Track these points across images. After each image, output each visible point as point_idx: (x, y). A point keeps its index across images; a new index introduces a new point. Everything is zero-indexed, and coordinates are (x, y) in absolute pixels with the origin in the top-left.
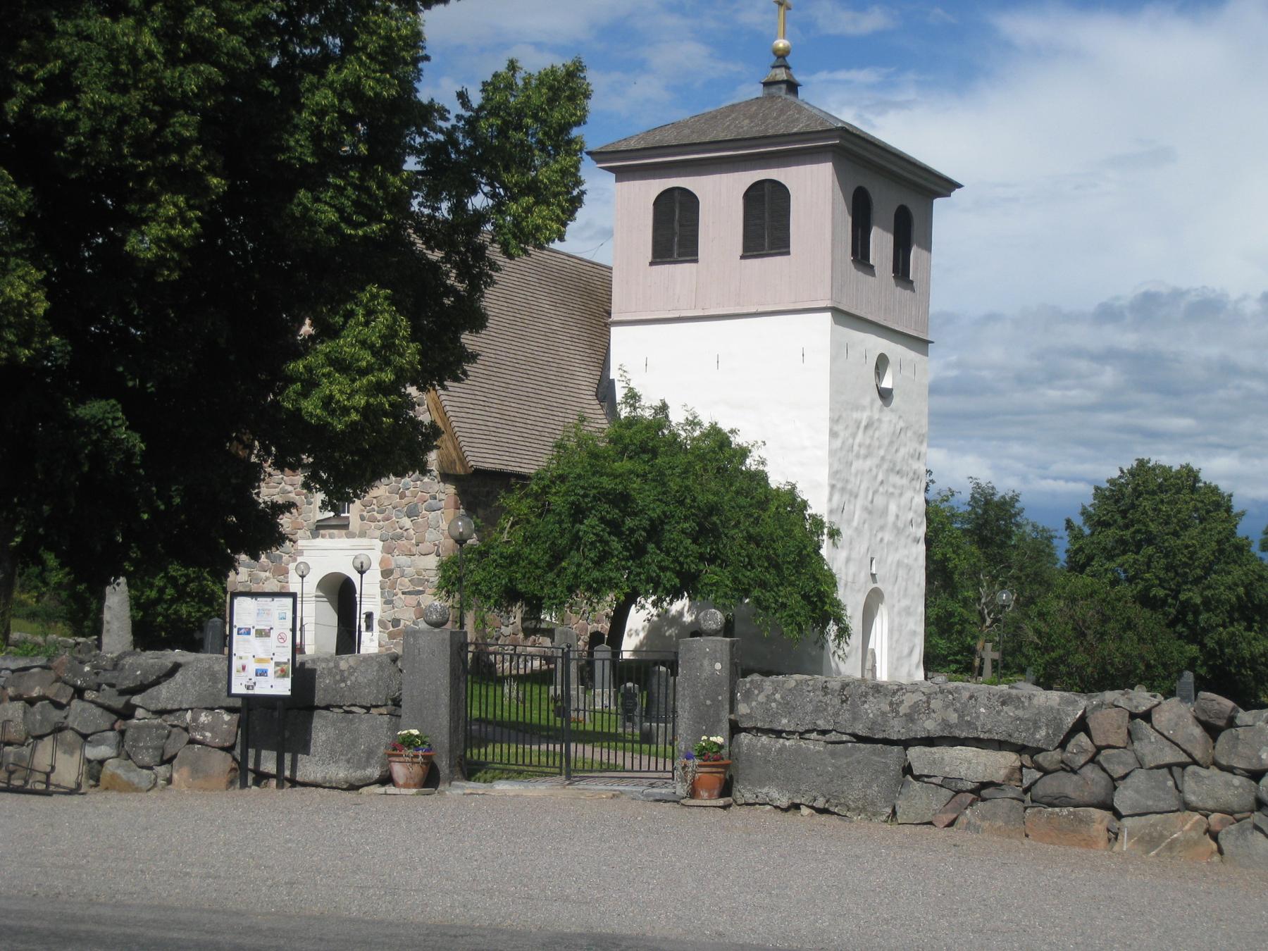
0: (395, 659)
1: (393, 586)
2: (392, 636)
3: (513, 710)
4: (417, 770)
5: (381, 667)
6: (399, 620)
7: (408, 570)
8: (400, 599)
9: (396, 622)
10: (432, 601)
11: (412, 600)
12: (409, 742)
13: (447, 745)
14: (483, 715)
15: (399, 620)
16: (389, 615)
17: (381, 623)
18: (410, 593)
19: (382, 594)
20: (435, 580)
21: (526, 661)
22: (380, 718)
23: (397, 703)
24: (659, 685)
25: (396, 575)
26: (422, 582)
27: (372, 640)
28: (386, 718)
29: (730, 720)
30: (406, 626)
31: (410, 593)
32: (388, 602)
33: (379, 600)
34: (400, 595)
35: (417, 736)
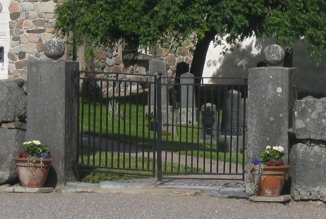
0: (21, 84)
1: (20, 26)
2: (18, 66)
3: (116, 125)
4: (39, 173)
5: (10, 90)
6: (24, 53)
7: (31, 13)
8: (25, 36)
9: (22, 55)
10: (50, 37)
11: (35, 37)
12: (32, 151)
13: (63, 153)
14: (92, 129)
15: (24, 53)
16: (17, 49)
17: (11, 56)
18: (33, 32)
19: (11, 32)
20: (53, 21)
21: (126, 86)
22: (9, 132)
23: (23, 119)
24: (232, 105)
25: (21, 17)
26: (42, 23)
27: (3, 69)
28: (14, 131)
29: (289, 133)
30: (30, 58)
31: (33, 32)
32: (16, 39)
33: (8, 37)
34: (25, 33)
35: (39, 146)
